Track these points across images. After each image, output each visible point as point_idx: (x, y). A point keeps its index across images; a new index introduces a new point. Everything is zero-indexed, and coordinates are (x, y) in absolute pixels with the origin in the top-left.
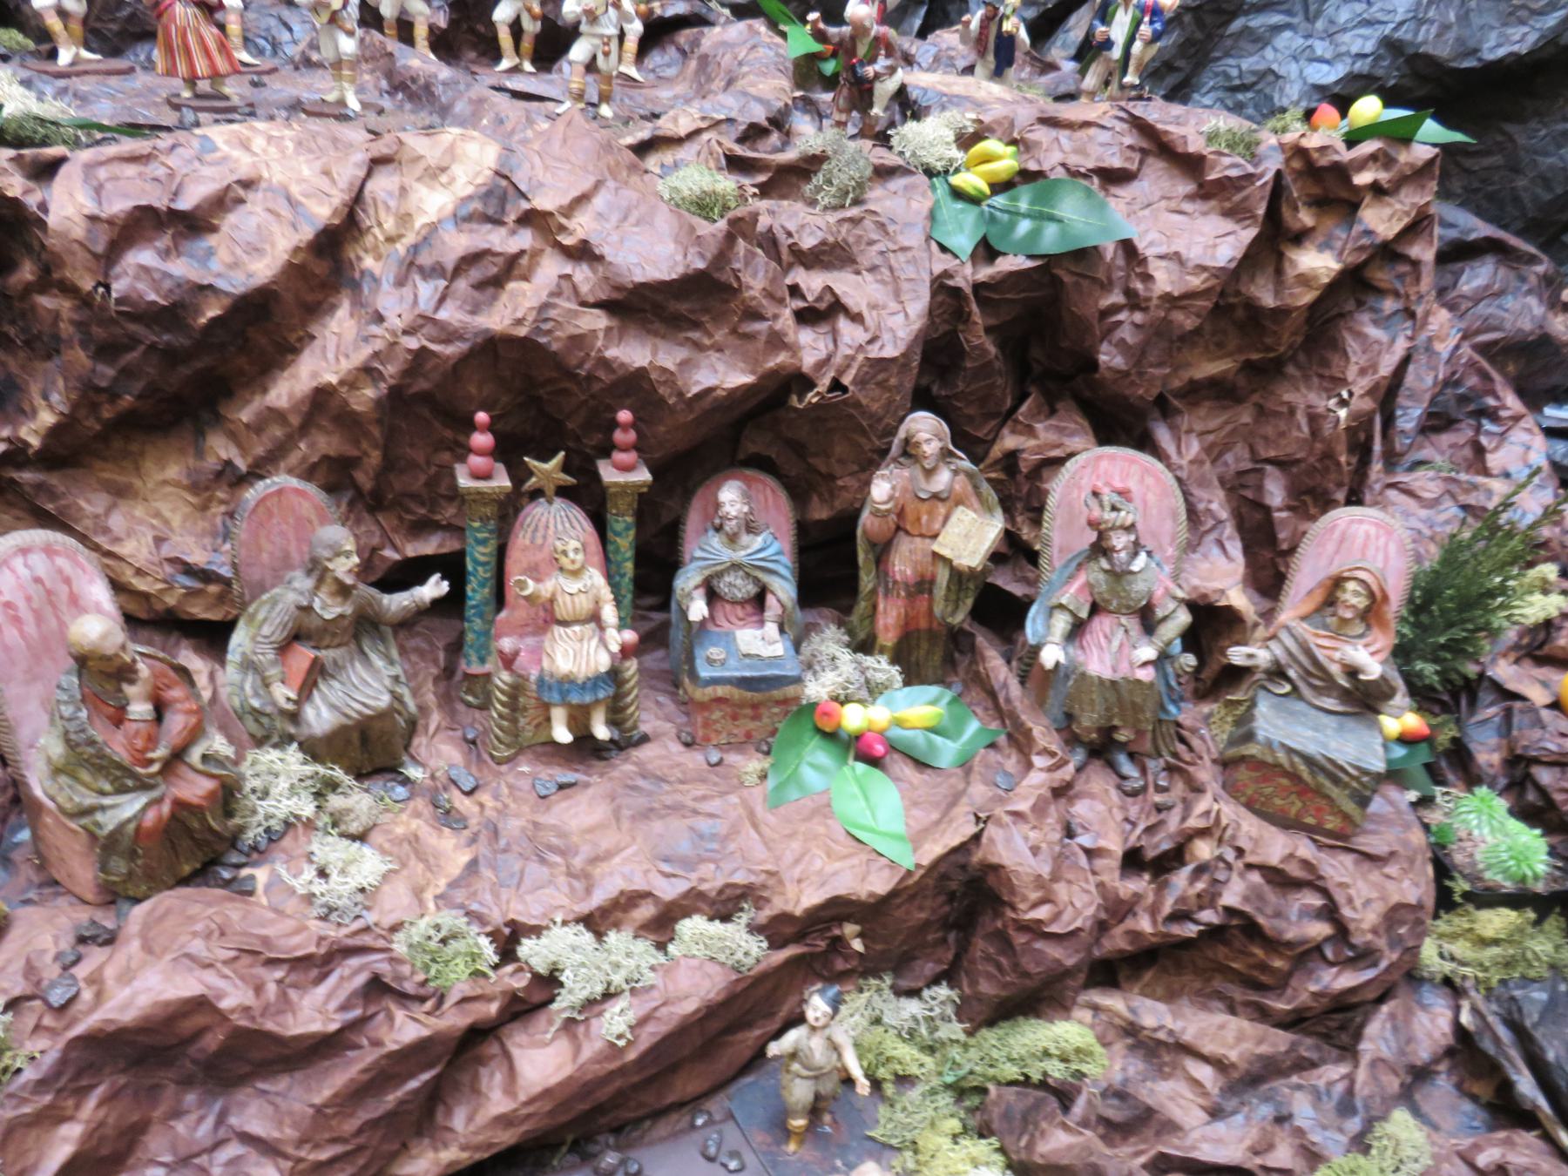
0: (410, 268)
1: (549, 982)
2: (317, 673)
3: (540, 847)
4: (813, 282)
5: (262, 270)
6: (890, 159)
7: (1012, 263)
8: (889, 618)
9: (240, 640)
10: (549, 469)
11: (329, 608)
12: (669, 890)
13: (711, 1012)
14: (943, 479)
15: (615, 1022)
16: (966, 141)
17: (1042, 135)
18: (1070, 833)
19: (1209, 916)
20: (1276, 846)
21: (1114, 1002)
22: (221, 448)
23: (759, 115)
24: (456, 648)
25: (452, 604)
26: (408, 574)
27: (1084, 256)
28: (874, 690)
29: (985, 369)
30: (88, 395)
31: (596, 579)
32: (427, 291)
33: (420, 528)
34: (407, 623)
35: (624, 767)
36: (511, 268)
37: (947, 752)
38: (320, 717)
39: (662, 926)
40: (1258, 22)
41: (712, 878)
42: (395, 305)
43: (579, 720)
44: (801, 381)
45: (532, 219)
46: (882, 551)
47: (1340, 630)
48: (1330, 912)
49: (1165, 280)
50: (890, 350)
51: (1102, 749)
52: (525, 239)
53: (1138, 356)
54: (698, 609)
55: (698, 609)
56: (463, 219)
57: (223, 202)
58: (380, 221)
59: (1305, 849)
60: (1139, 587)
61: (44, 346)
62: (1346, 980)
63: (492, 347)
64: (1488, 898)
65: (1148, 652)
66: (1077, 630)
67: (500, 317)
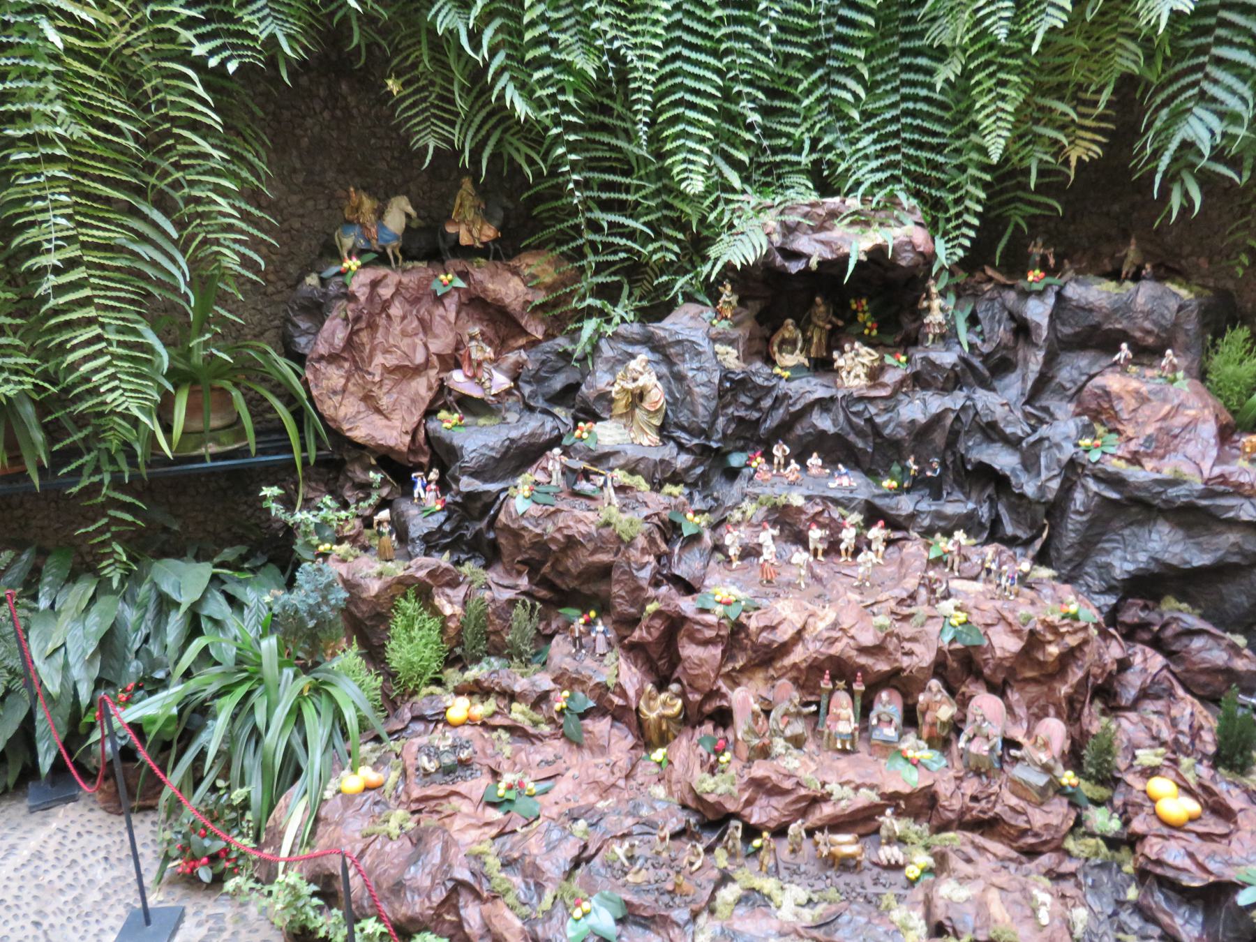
0: (815, 639)
1: (830, 794)
2: (788, 723)
3: (830, 768)
4: (907, 646)
5: (786, 637)
6: (934, 613)
7: (958, 646)
8: (925, 731)
9: (773, 714)
10: (841, 684)
11: (792, 710)
12: (859, 781)
13: (864, 809)
14: (939, 697)
15: (843, 804)
16: (957, 609)
17: (974, 611)
18: (958, 788)
19: (991, 814)
20: (1013, 801)
21: (969, 835)
22: (771, 672)
23: (905, 595)
24: (816, 724)
25: (817, 713)
26: (808, 704)
27: (977, 647)
28: (919, 749)
29: (953, 670)
30: (750, 660)
31: (850, 711)
32: (818, 644)
33: (812, 694)
34: (806, 716)
35: (853, 757)
36: (836, 640)
37: (935, 767)
38: (788, 733)
39: (857, 788)
40: (1107, 545)
41: (868, 781)
42: (811, 647)
43: (843, 742)
44: (901, 670)
45: (842, 629)
46: (924, 713)
47: (1039, 749)
48: (1028, 822)
49: (999, 653)
50: (924, 665)
51: (978, 773)
52: (839, 634)
53: (994, 671)
54: (874, 722)
55: (874, 722)
56: (827, 629)
57: (780, 623)
58: (810, 629)
59: (1023, 804)
60: (985, 731)
61: (744, 649)
62: (1031, 840)
63: (831, 657)
64: (1092, 835)
65: (987, 748)
66: (970, 740)
67: (835, 650)
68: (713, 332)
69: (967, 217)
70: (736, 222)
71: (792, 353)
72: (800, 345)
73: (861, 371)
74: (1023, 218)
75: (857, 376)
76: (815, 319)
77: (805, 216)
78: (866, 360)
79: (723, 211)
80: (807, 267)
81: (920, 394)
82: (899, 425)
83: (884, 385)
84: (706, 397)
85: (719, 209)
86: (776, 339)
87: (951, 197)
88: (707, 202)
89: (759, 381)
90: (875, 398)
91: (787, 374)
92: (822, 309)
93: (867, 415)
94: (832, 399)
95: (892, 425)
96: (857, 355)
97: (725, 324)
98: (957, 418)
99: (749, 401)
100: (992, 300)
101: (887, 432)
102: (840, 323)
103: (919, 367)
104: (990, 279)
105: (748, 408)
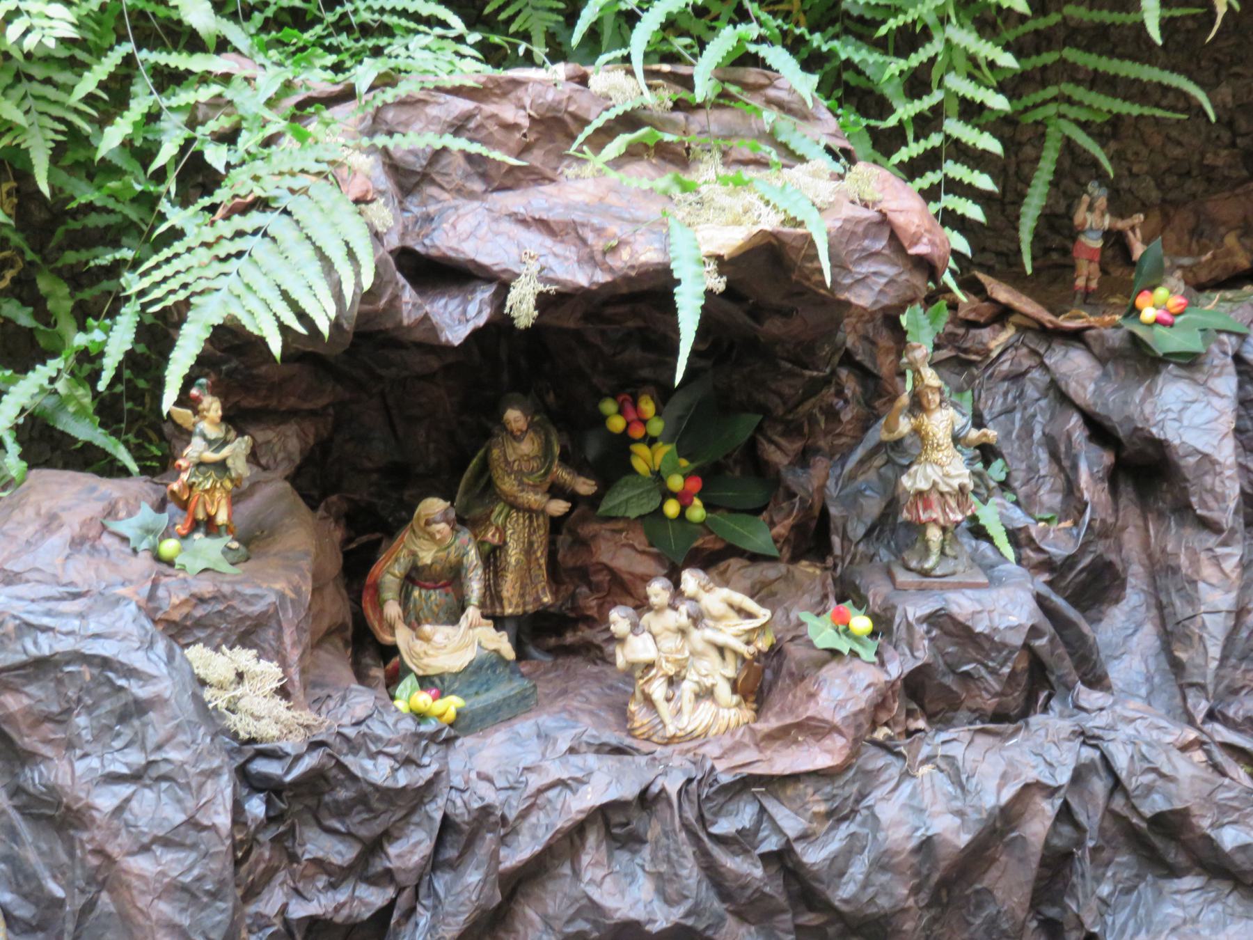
68: (173, 596)
69: (955, 128)
70: (216, 156)
71: (454, 615)
72: (475, 587)
73: (719, 673)
74: (1084, 126)
75: (705, 694)
76: (508, 485)
77: (458, 128)
78: (731, 632)
79: (152, 117)
80: (500, 325)
81: (937, 742)
82: (882, 864)
83: (815, 729)
84: (183, 892)
85: (139, 106)
86: (389, 573)
87: (897, 66)
88: (88, 83)
89: (379, 771)
90: (795, 778)
91: (451, 705)
92: (528, 447)
93: (771, 844)
94: (647, 800)
95: (858, 868)
96: (697, 619)
97: (208, 550)
98: (1065, 814)
99: (341, 853)
100: (1016, 377)
101: (844, 892)
102: (585, 487)
103: (924, 654)
104: (1003, 314)
105: (337, 876)
